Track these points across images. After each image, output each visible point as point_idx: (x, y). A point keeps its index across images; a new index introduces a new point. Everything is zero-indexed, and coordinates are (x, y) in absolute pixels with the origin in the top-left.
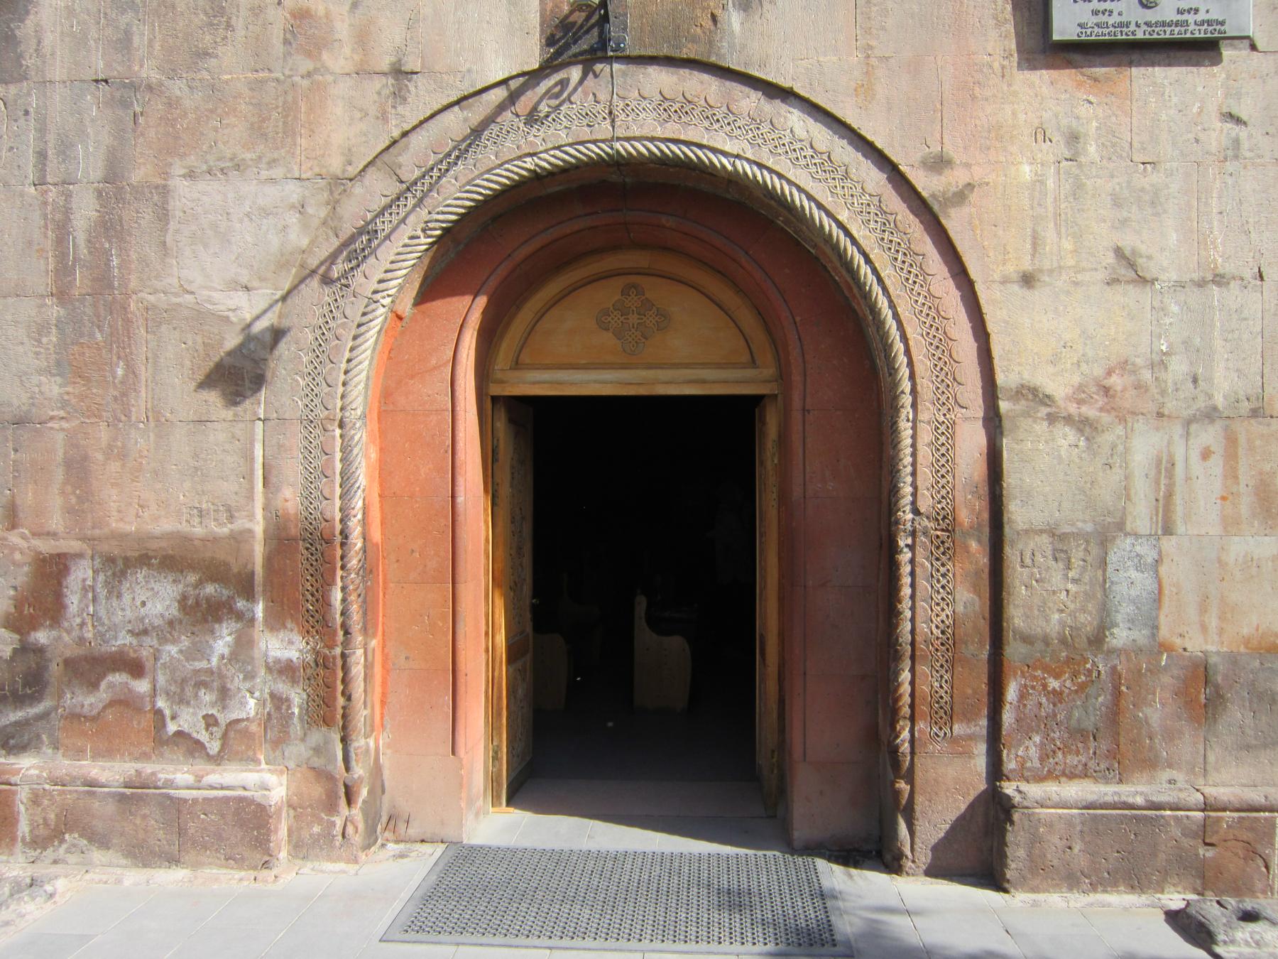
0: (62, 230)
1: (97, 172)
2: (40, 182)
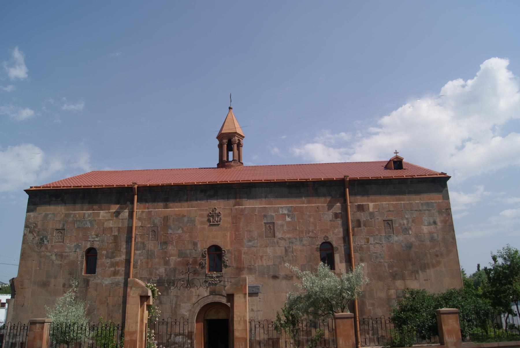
0: (172, 308)
2: (170, 303)
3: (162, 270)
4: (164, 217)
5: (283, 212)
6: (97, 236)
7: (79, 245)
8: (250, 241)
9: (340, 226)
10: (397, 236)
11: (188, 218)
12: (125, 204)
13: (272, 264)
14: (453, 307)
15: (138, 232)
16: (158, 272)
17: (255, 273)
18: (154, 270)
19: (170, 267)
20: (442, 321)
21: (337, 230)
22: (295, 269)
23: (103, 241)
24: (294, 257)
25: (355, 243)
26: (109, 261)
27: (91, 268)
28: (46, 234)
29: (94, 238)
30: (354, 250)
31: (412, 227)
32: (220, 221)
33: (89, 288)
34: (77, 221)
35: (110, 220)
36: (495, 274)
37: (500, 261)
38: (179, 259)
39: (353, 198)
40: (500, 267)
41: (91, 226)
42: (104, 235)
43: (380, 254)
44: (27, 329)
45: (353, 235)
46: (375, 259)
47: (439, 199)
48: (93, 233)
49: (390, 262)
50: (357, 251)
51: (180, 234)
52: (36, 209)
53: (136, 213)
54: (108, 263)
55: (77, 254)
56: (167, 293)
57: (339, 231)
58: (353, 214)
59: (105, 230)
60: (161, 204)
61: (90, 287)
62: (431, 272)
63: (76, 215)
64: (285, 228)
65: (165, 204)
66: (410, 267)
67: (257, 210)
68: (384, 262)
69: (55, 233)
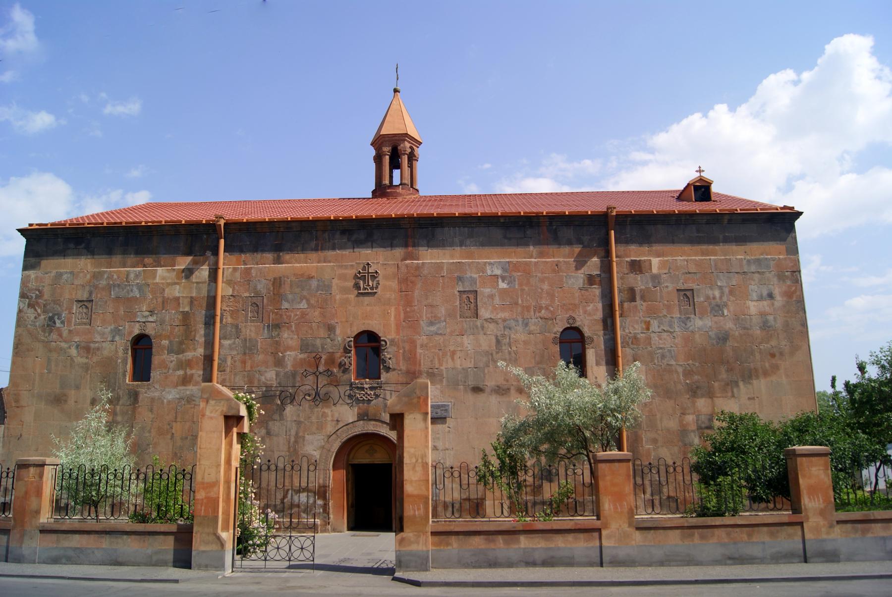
0: (289, 442)
1: (294, 434)
3: (270, 376)
4: (275, 279)
5: (492, 271)
6: (152, 312)
7: (119, 330)
8: (431, 324)
9: (598, 299)
10: (700, 318)
11: (318, 281)
12: (200, 256)
13: (472, 365)
14: (815, 442)
15: (228, 306)
16: (263, 379)
17: (441, 381)
18: (257, 376)
19: (286, 370)
20: (799, 469)
21: (592, 305)
22: (517, 371)
23: (162, 322)
24: (513, 355)
25: (624, 331)
26: (174, 358)
27: (142, 372)
28: (59, 309)
29: (146, 317)
30: (622, 343)
31: (729, 303)
32: (377, 288)
33: (139, 406)
34: (114, 286)
36: (862, 393)
37: (873, 372)
38: (302, 356)
39: (622, 248)
40: (875, 381)
41: (140, 295)
43: (670, 351)
44: (13, 477)
45: (621, 316)
46: (660, 359)
47: (780, 253)
48: (145, 307)
49: (688, 364)
50: (628, 345)
51: (304, 310)
52: (39, 263)
53: (223, 273)
54: (172, 362)
55: (116, 346)
56: (281, 415)
57: (596, 309)
58: (622, 278)
59: (167, 302)
60: (269, 256)
61: (140, 404)
62: (761, 385)
63: (113, 275)
64: (497, 301)
65: (276, 255)
66: (724, 375)
67: (445, 268)
68: (677, 364)
69: (75, 308)
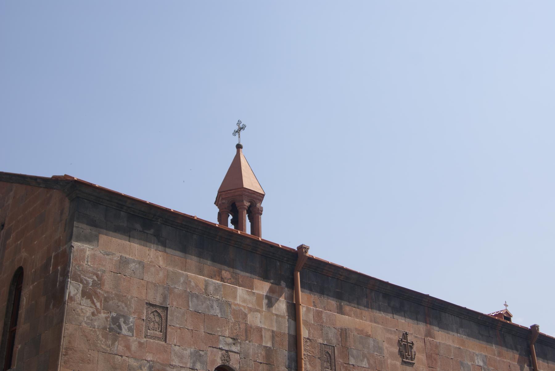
5: (478, 362)
7: (200, 355)
11: (374, 341)
28: (126, 309)
29: (229, 344)
35: (257, 311)
41: (221, 314)
42: (247, 342)
48: (227, 332)
52: (96, 238)
60: (333, 303)
63: (190, 281)
